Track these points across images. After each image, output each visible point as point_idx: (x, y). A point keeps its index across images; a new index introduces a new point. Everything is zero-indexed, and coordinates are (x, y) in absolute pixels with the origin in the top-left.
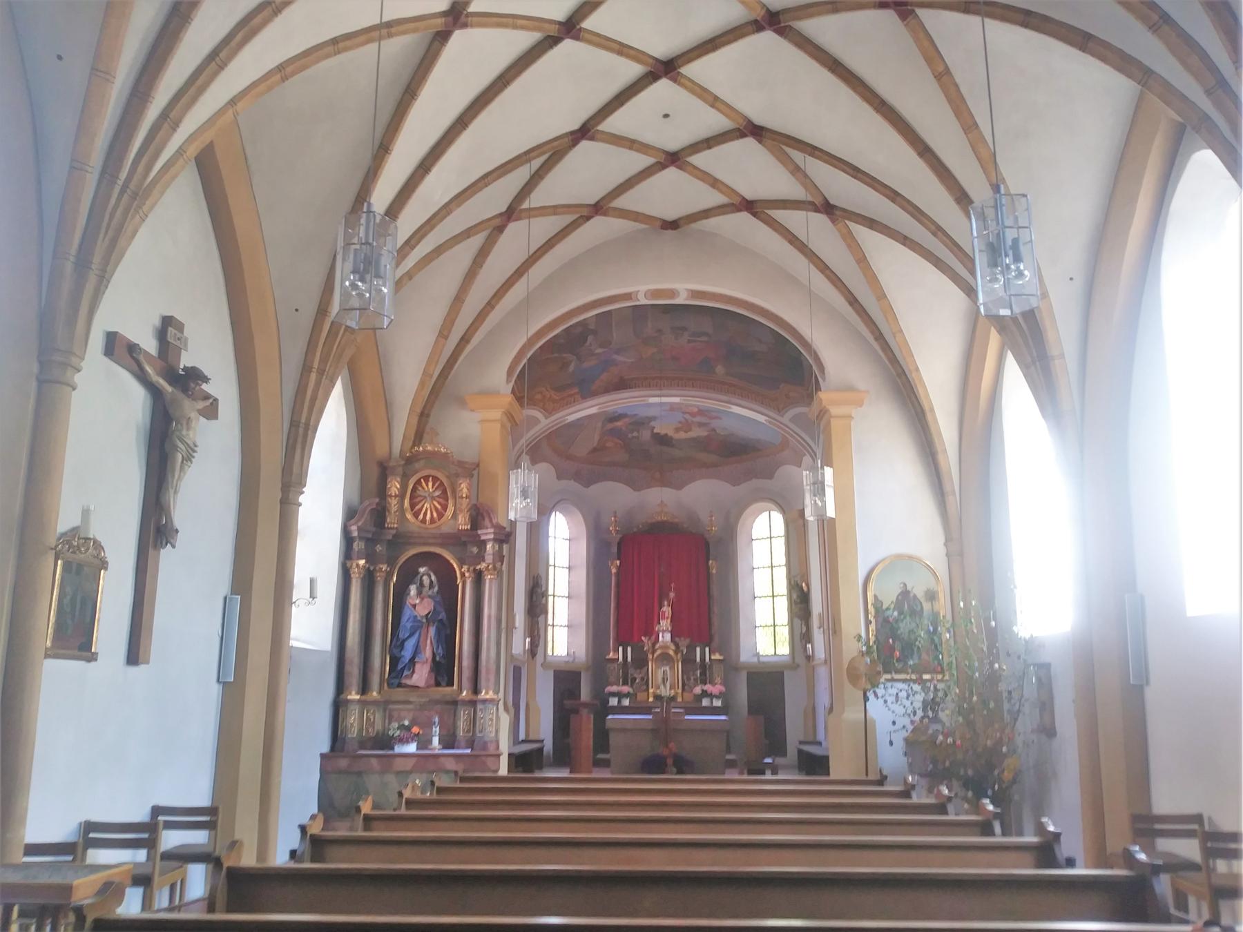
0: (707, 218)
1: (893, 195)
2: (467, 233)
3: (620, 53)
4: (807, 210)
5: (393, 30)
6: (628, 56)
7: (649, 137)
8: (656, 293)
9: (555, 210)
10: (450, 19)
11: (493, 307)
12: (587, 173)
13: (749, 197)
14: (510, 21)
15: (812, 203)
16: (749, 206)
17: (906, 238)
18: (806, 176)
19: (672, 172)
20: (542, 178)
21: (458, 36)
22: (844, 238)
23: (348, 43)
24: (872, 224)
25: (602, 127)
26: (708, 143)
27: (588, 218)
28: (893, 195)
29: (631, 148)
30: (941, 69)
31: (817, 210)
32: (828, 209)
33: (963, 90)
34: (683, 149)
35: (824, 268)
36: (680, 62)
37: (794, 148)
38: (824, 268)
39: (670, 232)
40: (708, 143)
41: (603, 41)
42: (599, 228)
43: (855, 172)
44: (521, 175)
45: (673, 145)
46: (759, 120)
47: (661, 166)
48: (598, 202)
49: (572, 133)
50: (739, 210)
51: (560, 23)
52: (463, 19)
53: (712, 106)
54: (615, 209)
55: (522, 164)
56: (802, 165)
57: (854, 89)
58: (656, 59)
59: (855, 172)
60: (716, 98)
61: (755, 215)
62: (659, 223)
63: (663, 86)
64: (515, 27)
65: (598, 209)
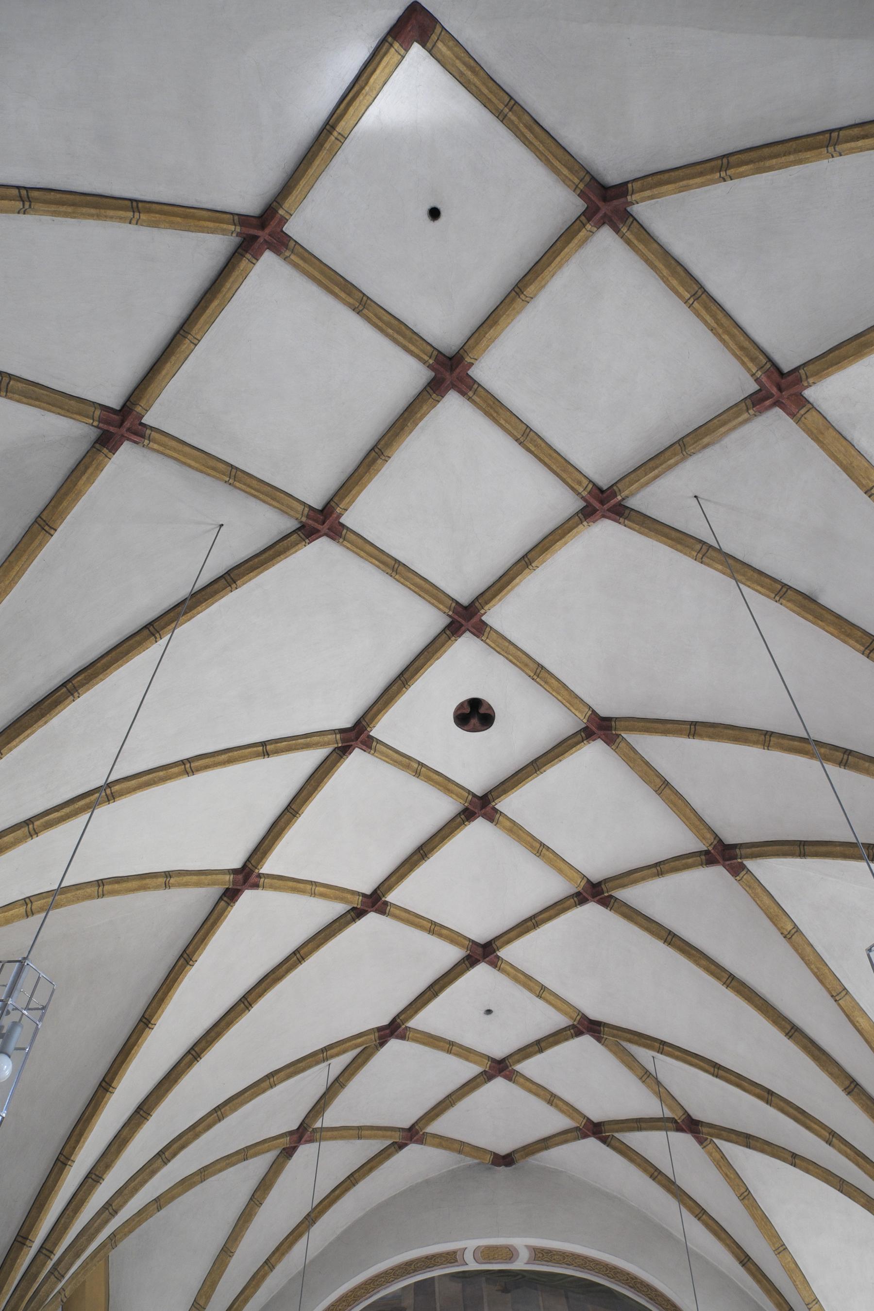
0: (547, 1148)
1: (768, 1096)
2: (244, 1154)
3: (431, 932)
4: (666, 1129)
5: (172, 881)
6: (440, 936)
7: (468, 1040)
8: (488, 1253)
9: (359, 1132)
10: (240, 877)
11: (272, 1268)
12: (397, 1086)
13: (596, 1117)
14: (309, 887)
15: (673, 1121)
16: (596, 1130)
17: (794, 1155)
18: (659, 1083)
19: (499, 1084)
20: (343, 1086)
21: (248, 896)
22: (719, 1167)
23: (116, 886)
24: (748, 1140)
25: (412, 1024)
26: (539, 1046)
27: (401, 1146)
28: (768, 1096)
29: (449, 1052)
30: (789, 927)
31: (679, 1129)
32: (691, 1125)
33: (819, 949)
34: (511, 1055)
35: (700, 1213)
36: (498, 943)
37: (640, 1045)
38: (700, 1213)
39: (502, 1168)
40: (539, 1046)
41: (412, 918)
42: (416, 1161)
43: (716, 1069)
44: (314, 1081)
45: (499, 1051)
46: (594, 1014)
47: (487, 1076)
48: (413, 1126)
49: (380, 1029)
50: (585, 1136)
51: (364, 895)
52: (253, 879)
53: (539, 996)
54: (435, 1136)
55: (318, 1063)
56: (651, 1068)
57: (697, 962)
58: (473, 942)
59: (716, 1069)
60: (543, 988)
61: (604, 1140)
62: (488, 1158)
63: (482, 970)
64: (313, 894)
65: (413, 1134)
